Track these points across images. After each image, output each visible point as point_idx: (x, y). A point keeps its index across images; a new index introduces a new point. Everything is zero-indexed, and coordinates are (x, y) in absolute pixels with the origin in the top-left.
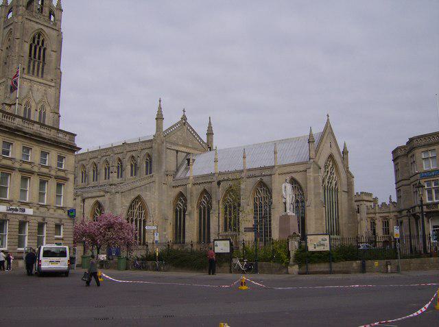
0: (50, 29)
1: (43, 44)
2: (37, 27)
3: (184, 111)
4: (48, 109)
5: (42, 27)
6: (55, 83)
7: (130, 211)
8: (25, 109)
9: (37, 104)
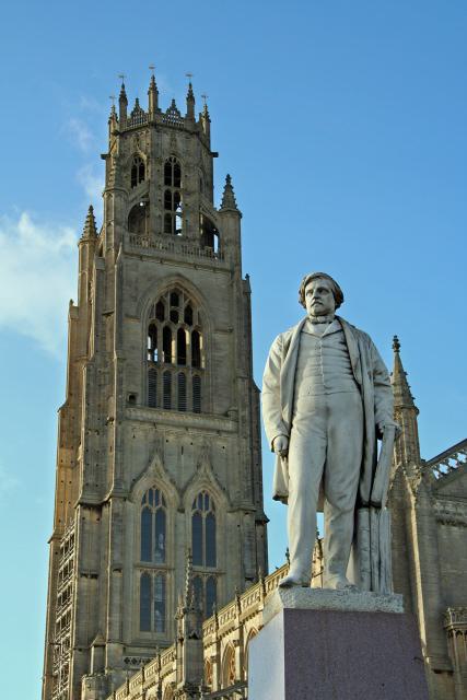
0: (201, 272)
1: (189, 321)
4: (221, 501)
5: (181, 270)
6: (236, 421)
8: (146, 513)
9: (182, 492)
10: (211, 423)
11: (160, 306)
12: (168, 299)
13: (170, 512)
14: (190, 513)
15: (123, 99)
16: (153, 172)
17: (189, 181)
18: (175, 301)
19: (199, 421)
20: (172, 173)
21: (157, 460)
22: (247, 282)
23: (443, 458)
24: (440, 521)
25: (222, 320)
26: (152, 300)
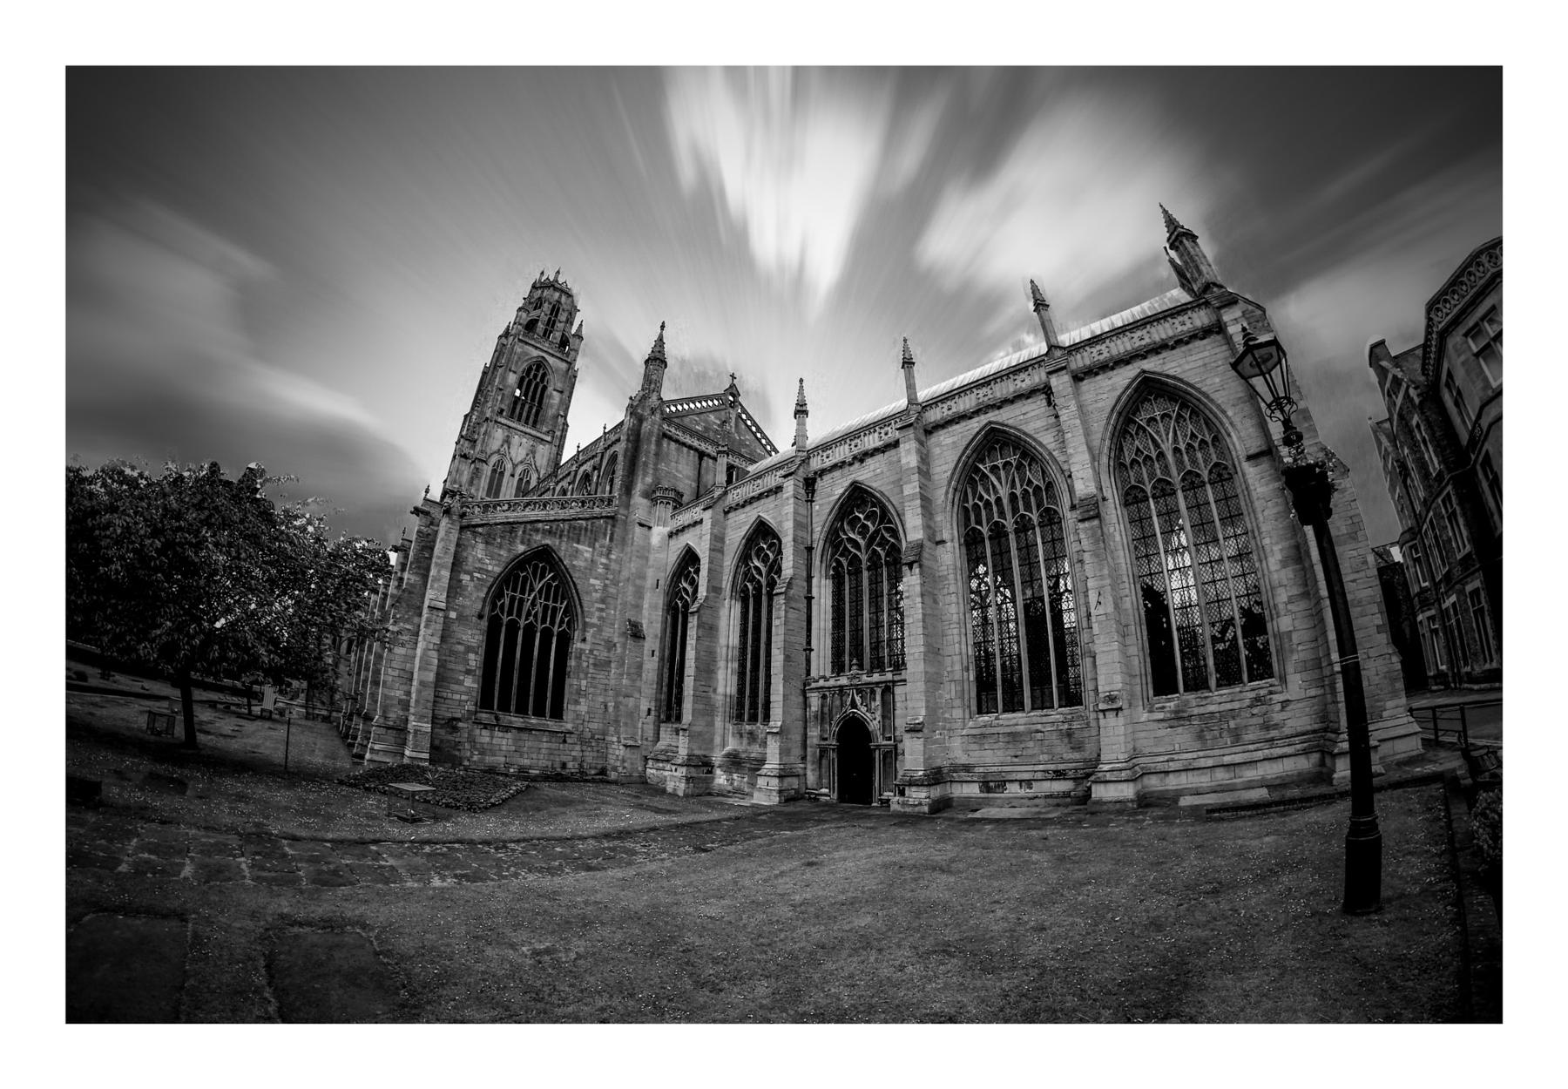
2: (535, 353)
3: (733, 377)
6: (553, 437)
7: (508, 593)
8: (494, 471)
9: (515, 466)
10: (539, 435)
11: (530, 369)
12: (534, 367)
13: (507, 474)
14: (517, 478)
15: (542, 273)
16: (546, 307)
17: (563, 317)
18: (537, 370)
19: (534, 433)
20: (555, 310)
21: (506, 446)
22: (576, 372)
23: (674, 402)
24: (665, 435)
25: (559, 386)
26: (525, 365)
